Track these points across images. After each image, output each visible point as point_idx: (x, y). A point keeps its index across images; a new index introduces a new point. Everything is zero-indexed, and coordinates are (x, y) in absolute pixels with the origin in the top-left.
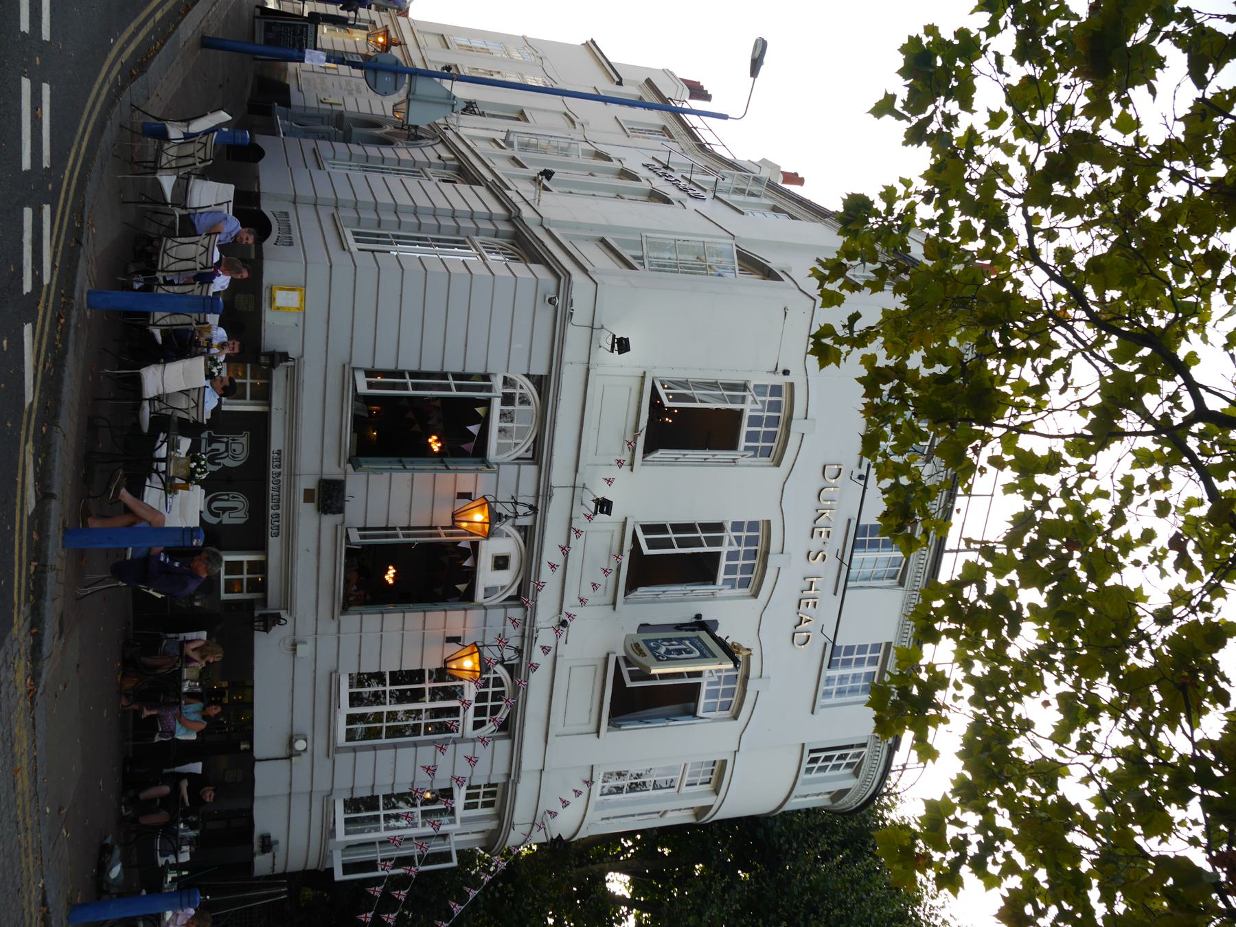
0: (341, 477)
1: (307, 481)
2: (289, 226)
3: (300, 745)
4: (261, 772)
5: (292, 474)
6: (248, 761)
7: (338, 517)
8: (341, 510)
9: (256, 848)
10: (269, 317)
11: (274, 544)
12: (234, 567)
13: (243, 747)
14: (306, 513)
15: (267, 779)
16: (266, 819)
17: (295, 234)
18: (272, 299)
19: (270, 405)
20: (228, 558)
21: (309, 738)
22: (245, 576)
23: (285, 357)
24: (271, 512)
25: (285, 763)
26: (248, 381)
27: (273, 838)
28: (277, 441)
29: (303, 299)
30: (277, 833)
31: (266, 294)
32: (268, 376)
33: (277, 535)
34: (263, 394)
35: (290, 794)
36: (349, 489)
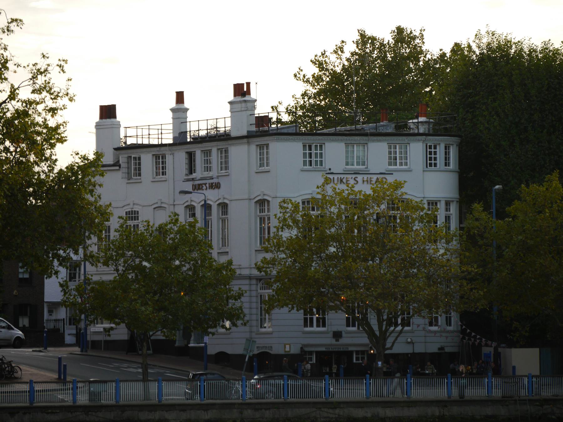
0: (332, 332)
1: (333, 341)
2: (263, 347)
3: (409, 340)
4: (417, 351)
5: (331, 345)
6: (414, 354)
7: (343, 333)
8: (341, 332)
9: (443, 351)
10: (292, 352)
11: (351, 349)
12: (357, 359)
13: (409, 356)
14: (342, 341)
15: (419, 349)
16: (433, 349)
17: (270, 345)
18: (288, 352)
19: (313, 351)
20: (355, 361)
21: (407, 338)
22: (360, 356)
23: (302, 348)
24: (342, 350)
25: (415, 344)
26: (307, 356)
27: (440, 347)
28: (323, 349)
29: (287, 344)
30: (439, 346)
31: (286, 353)
32: (306, 351)
33: (348, 348)
34: (311, 353)
35: (425, 342)
36: (335, 330)
